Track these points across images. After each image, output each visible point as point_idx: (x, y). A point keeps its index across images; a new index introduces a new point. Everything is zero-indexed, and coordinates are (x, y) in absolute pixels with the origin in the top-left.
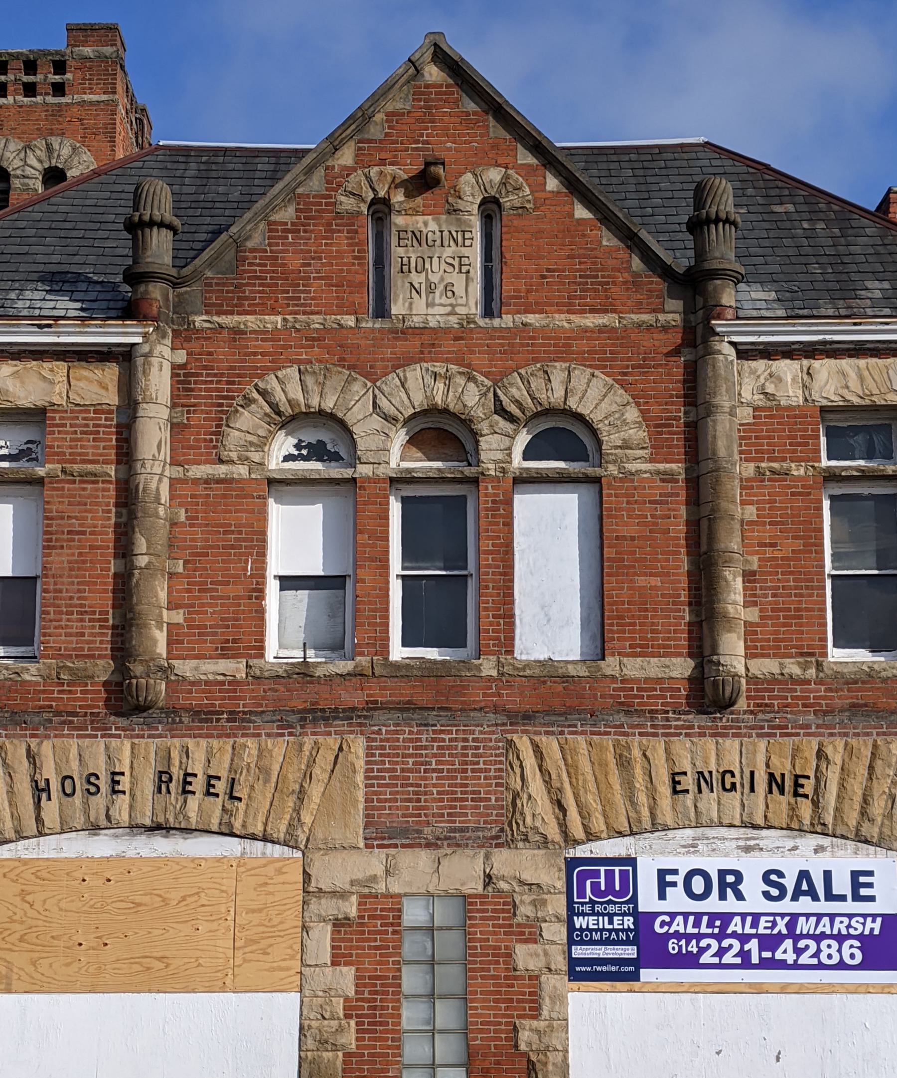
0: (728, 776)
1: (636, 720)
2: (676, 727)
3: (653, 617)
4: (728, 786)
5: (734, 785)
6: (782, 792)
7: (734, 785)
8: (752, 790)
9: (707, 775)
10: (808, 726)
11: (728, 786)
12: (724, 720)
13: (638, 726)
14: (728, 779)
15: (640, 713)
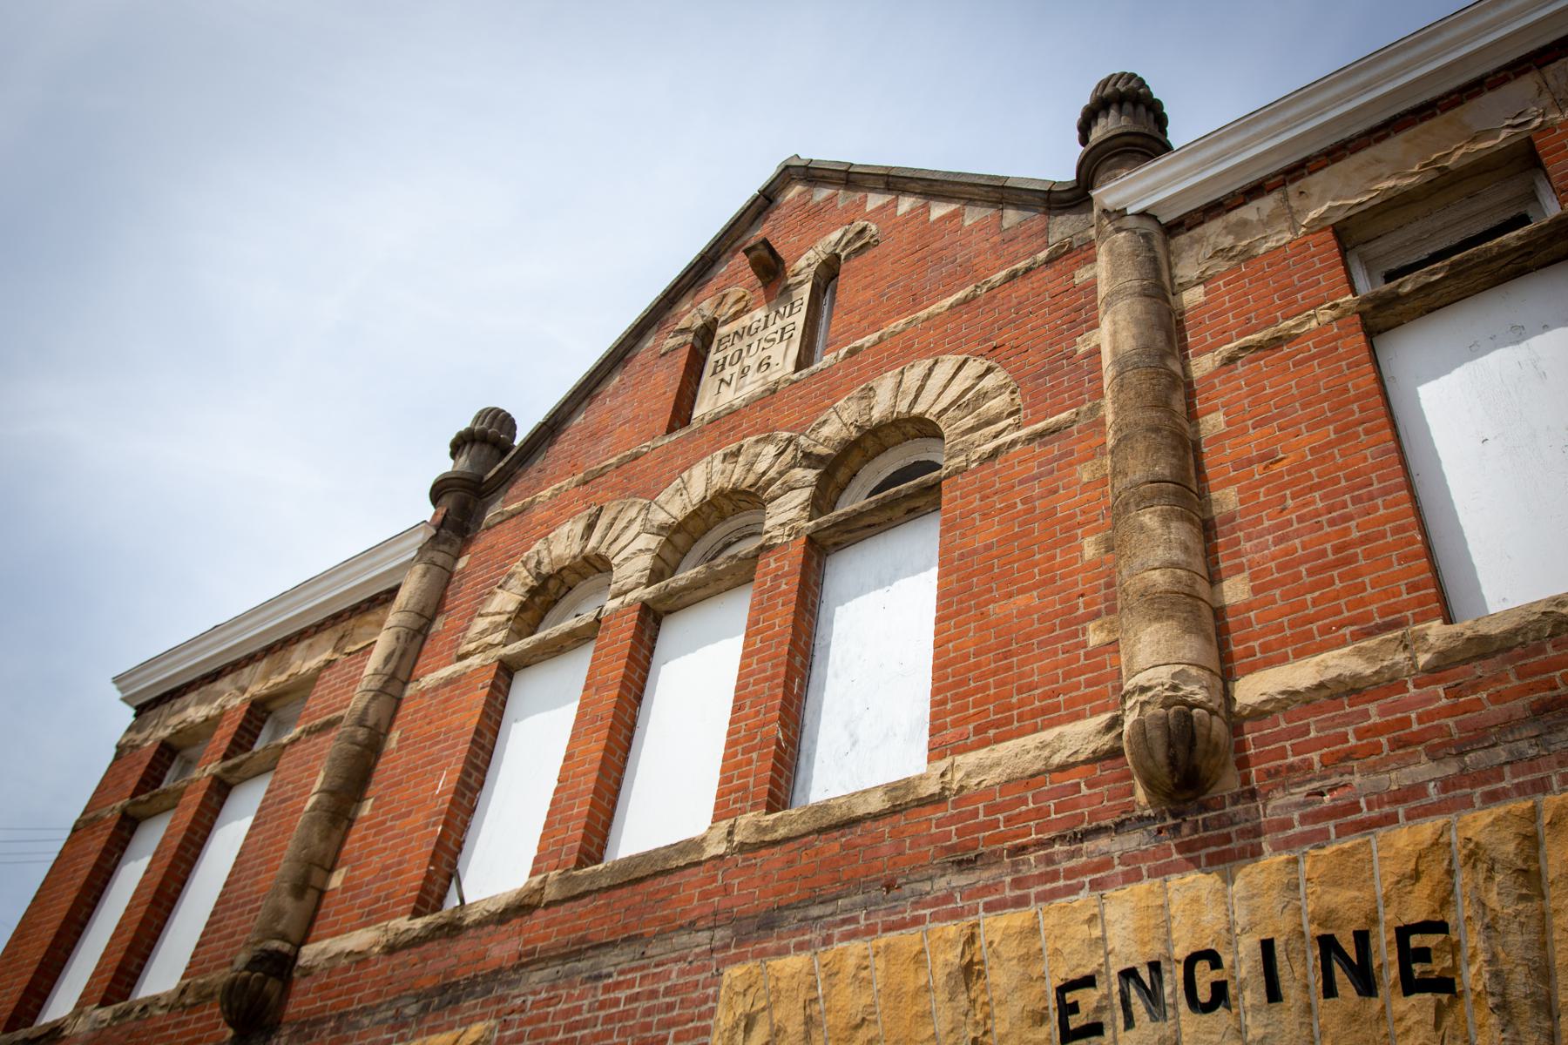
0: (1202, 967)
1: (981, 876)
2: (1070, 874)
3: (1022, 664)
4: (1204, 995)
5: (1220, 993)
6: (1366, 983)
7: (1219, 990)
8: (1274, 993)
9: (1145, 974)
10: (1417, 790)
11: (1204, 995)
12: (1185, 829)
13: (987, 890)
14: (1205, 976)
15: (992, 859)
